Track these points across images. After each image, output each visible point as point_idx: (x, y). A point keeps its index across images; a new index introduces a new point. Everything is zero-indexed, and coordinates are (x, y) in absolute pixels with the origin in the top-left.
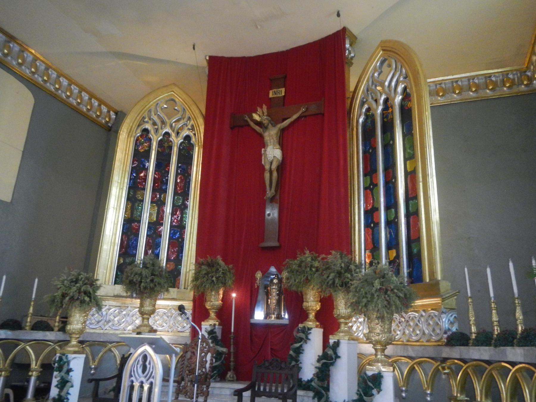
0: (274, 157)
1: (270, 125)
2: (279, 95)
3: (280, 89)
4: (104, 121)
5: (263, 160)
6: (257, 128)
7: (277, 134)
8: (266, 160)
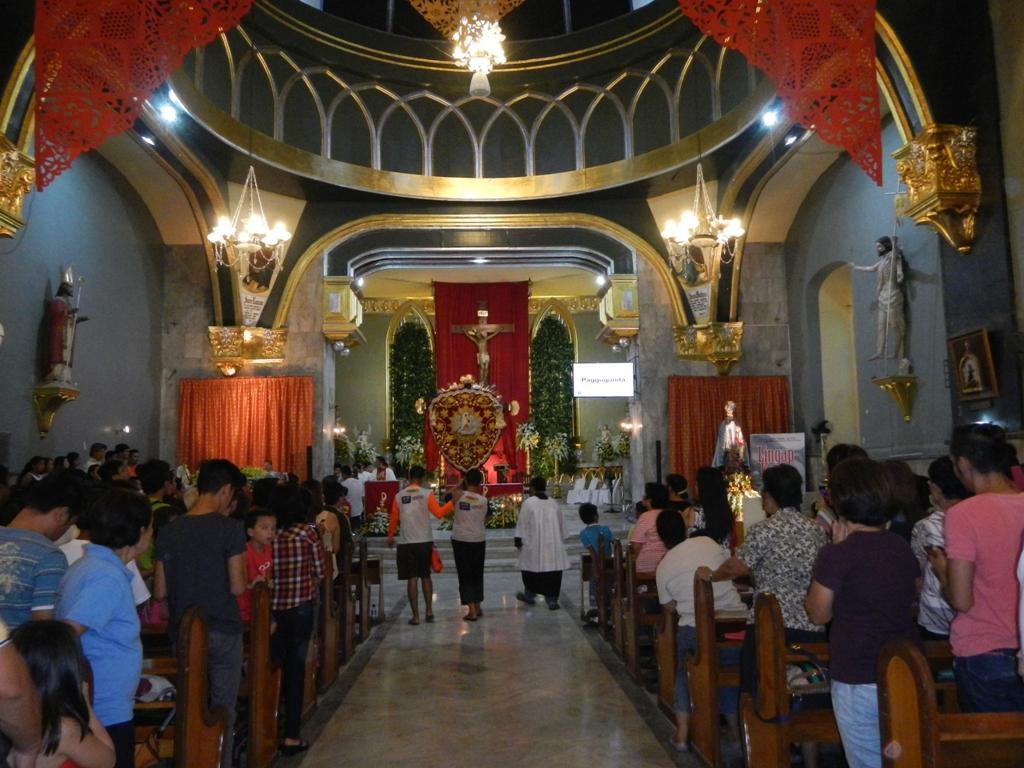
6: (472, 339)
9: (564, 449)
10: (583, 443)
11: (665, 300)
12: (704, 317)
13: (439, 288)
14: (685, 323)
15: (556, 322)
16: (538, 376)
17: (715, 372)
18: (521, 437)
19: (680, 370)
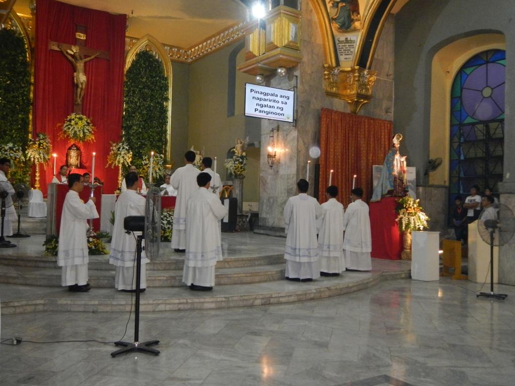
6: (70, 57)
9: (161, 168)
11: (319, 41)
12: (348, 62)
14: (334, 64)
15: (151, 56)
16: (132, 102)
17: (348, 110)
18: (116, 155)
19: (327, 103)
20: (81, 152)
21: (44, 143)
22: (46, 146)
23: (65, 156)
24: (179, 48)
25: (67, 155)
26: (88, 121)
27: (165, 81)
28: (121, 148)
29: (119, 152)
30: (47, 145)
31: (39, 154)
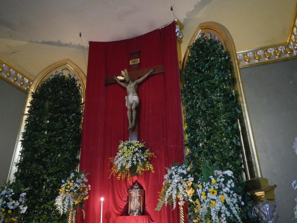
0: (133, 101)
1: (130, 81)
2: (136, 63)
3: (136, 59)
4: (26, 89)
5: (126, 104)
6: (122, 84)
7: (135, 86)
8: (128, 103)
9: (228, 200)
10: (269, 190)
13: (96, 49)
20: (145, 191)
21: (71, 184)
22: (76, 188)
23: (126, 199)
24: (276, 47)
25: (129, 199)
26: (141, 146)
27: (225, 57)
28: (174, 173)
29: (170, 181)
30: (78, 186)
31: (64, 200)
